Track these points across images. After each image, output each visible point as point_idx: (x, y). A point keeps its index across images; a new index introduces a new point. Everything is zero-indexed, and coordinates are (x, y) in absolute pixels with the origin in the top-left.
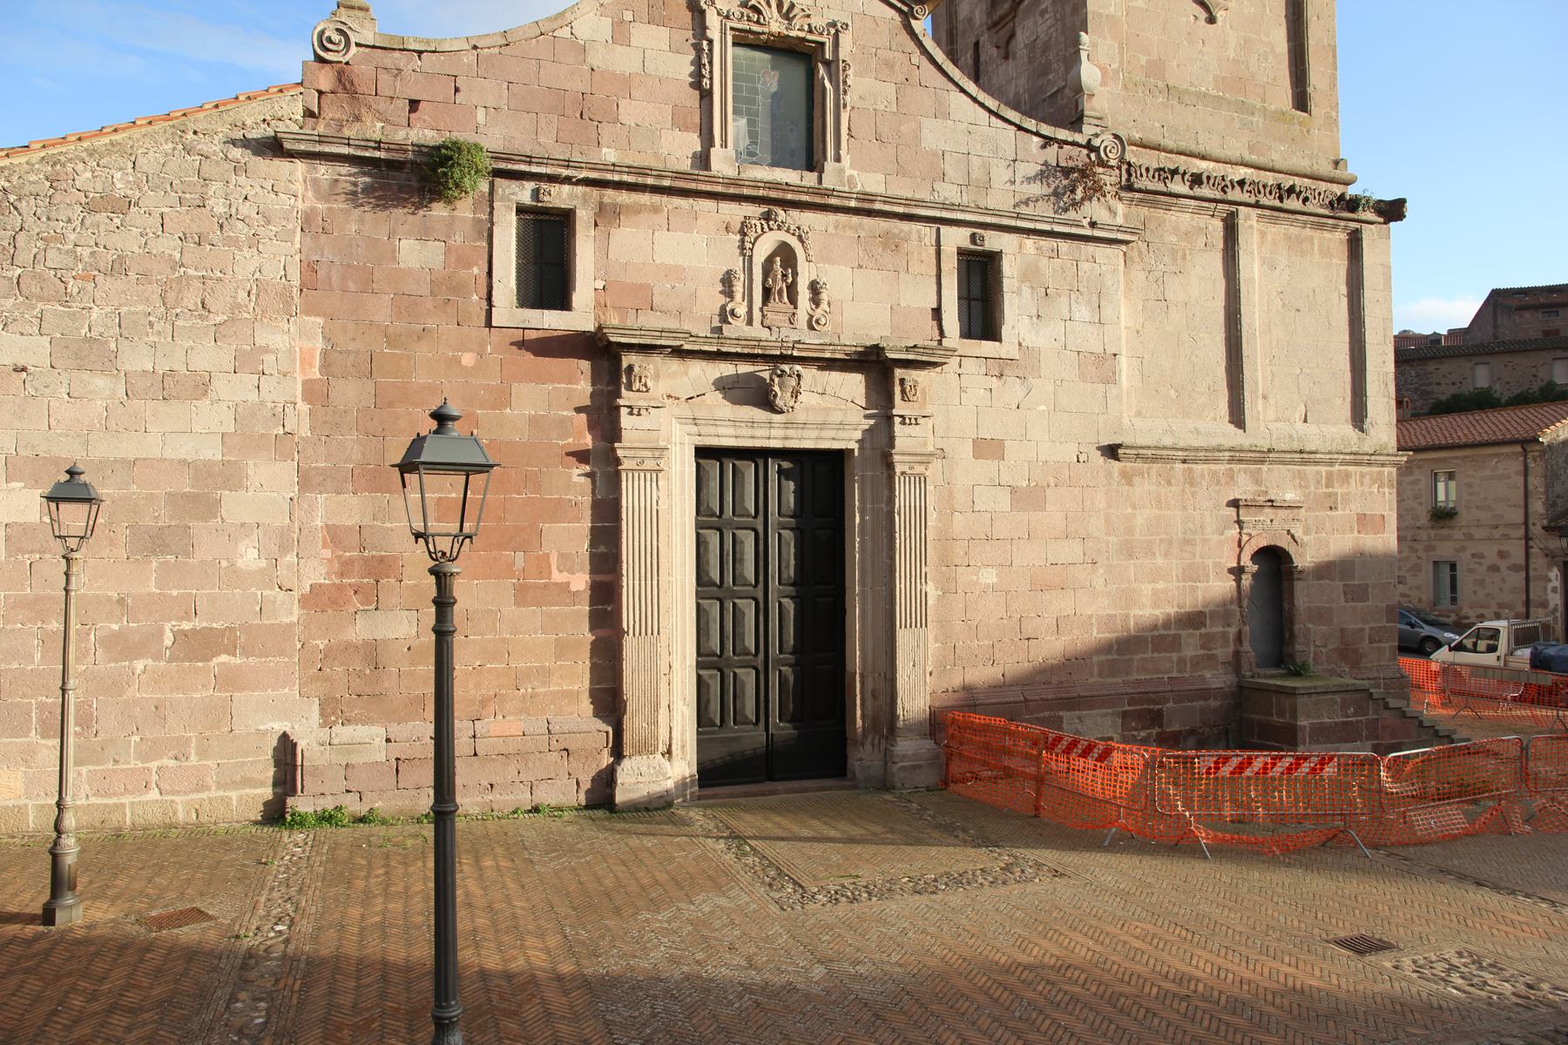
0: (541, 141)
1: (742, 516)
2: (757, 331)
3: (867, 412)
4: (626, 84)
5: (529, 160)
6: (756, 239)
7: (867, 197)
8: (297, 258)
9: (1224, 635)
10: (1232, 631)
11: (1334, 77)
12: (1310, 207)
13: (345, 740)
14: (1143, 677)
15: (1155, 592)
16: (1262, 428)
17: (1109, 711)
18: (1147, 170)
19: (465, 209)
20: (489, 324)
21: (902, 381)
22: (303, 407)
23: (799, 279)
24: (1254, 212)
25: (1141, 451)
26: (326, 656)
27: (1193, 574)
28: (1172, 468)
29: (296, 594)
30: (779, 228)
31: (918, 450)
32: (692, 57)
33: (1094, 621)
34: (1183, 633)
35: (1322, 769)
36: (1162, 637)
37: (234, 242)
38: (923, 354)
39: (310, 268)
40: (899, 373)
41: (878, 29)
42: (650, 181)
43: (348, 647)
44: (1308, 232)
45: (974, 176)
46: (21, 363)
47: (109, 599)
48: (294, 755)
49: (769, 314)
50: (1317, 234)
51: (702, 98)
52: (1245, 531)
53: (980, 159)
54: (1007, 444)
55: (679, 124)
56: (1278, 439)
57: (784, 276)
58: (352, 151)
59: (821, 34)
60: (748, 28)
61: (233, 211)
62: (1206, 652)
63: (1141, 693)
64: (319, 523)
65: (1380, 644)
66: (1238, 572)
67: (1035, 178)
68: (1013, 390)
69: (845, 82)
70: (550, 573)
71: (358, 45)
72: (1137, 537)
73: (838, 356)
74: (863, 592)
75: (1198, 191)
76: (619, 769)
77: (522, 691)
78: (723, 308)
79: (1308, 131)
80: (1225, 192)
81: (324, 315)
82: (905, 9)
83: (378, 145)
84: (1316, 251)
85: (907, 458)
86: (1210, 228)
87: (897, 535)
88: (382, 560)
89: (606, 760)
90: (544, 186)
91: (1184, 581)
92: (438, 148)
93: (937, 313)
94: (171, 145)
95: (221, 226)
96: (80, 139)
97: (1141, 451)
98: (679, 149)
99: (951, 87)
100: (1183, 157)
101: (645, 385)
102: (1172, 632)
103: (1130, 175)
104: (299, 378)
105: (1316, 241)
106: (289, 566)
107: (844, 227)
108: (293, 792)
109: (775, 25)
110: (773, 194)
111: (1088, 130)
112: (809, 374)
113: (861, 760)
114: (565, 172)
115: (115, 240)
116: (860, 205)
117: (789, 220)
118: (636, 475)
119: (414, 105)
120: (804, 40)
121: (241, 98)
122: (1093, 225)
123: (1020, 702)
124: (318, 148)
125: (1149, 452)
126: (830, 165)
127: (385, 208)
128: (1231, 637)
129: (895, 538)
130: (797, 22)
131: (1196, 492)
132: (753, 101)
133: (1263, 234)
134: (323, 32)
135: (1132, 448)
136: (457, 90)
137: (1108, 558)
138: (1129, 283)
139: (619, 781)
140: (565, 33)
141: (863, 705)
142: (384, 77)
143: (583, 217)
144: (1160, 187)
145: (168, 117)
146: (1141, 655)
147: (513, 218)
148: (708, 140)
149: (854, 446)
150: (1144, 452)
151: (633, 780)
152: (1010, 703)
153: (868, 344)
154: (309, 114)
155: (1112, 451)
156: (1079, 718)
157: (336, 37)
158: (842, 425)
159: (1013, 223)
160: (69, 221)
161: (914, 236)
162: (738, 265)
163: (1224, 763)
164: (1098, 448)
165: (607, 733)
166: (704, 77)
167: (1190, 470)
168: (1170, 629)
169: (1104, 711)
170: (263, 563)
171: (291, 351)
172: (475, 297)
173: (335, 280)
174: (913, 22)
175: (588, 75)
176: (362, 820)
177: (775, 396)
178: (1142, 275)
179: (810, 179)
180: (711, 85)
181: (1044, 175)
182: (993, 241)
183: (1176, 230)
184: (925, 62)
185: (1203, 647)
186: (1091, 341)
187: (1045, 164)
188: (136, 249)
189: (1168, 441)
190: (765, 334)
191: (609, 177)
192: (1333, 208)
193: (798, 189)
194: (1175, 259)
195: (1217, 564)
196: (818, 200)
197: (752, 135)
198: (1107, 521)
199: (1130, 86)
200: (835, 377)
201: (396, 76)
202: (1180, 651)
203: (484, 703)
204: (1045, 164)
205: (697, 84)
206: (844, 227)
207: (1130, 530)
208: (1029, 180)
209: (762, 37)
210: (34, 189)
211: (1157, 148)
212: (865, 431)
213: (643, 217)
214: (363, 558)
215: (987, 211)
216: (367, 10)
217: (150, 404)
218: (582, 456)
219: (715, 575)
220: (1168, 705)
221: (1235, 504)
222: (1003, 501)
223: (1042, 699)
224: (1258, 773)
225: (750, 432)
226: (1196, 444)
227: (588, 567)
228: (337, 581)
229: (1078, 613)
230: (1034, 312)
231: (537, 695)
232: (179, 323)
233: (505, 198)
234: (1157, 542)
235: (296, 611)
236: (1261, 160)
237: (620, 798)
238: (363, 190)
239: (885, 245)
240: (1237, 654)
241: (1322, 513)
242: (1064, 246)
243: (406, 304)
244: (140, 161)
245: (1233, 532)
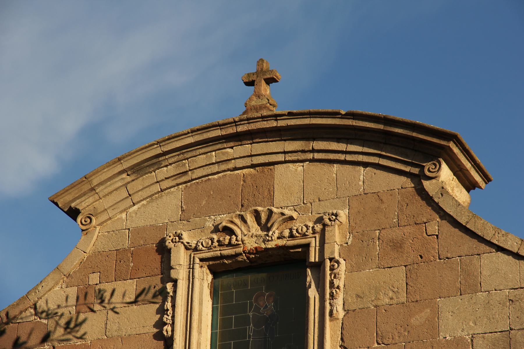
41: (383, 206)
60: (218, 253)
69: (332, 283)
82: (416, 171)
99: (483, 247)
130: (275, 232)
166: (165, 324)
174: (426, 184)
180: (173, 331)
184: (446, 226)
209: (240, 259)
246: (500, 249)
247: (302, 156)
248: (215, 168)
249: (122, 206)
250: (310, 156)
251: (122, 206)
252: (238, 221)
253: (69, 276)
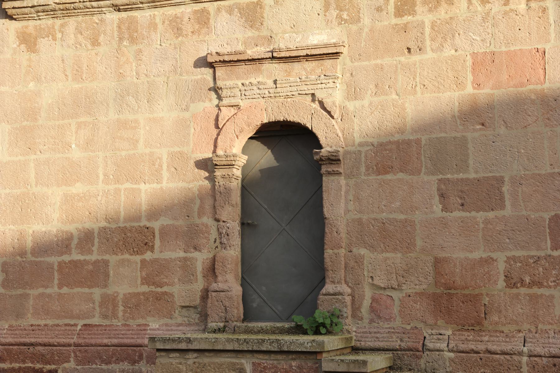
14: (42, 323)
28: (101, 20)
34: (113, 259)
36: (75, 264)
52: (225, 102)
62: (153, 288)
63: (24, 344)
65: (535, 290)
72: (40, 122)
102: (93, 257)
128: (199, 268)
131: (140, 51)
146: (41, 290)
167: (133, 21)
168: (90, 252)
185: (146, 281)
202: (106, 286)
220: (66, 365)
241: (387, 61)
245: (207, 104)
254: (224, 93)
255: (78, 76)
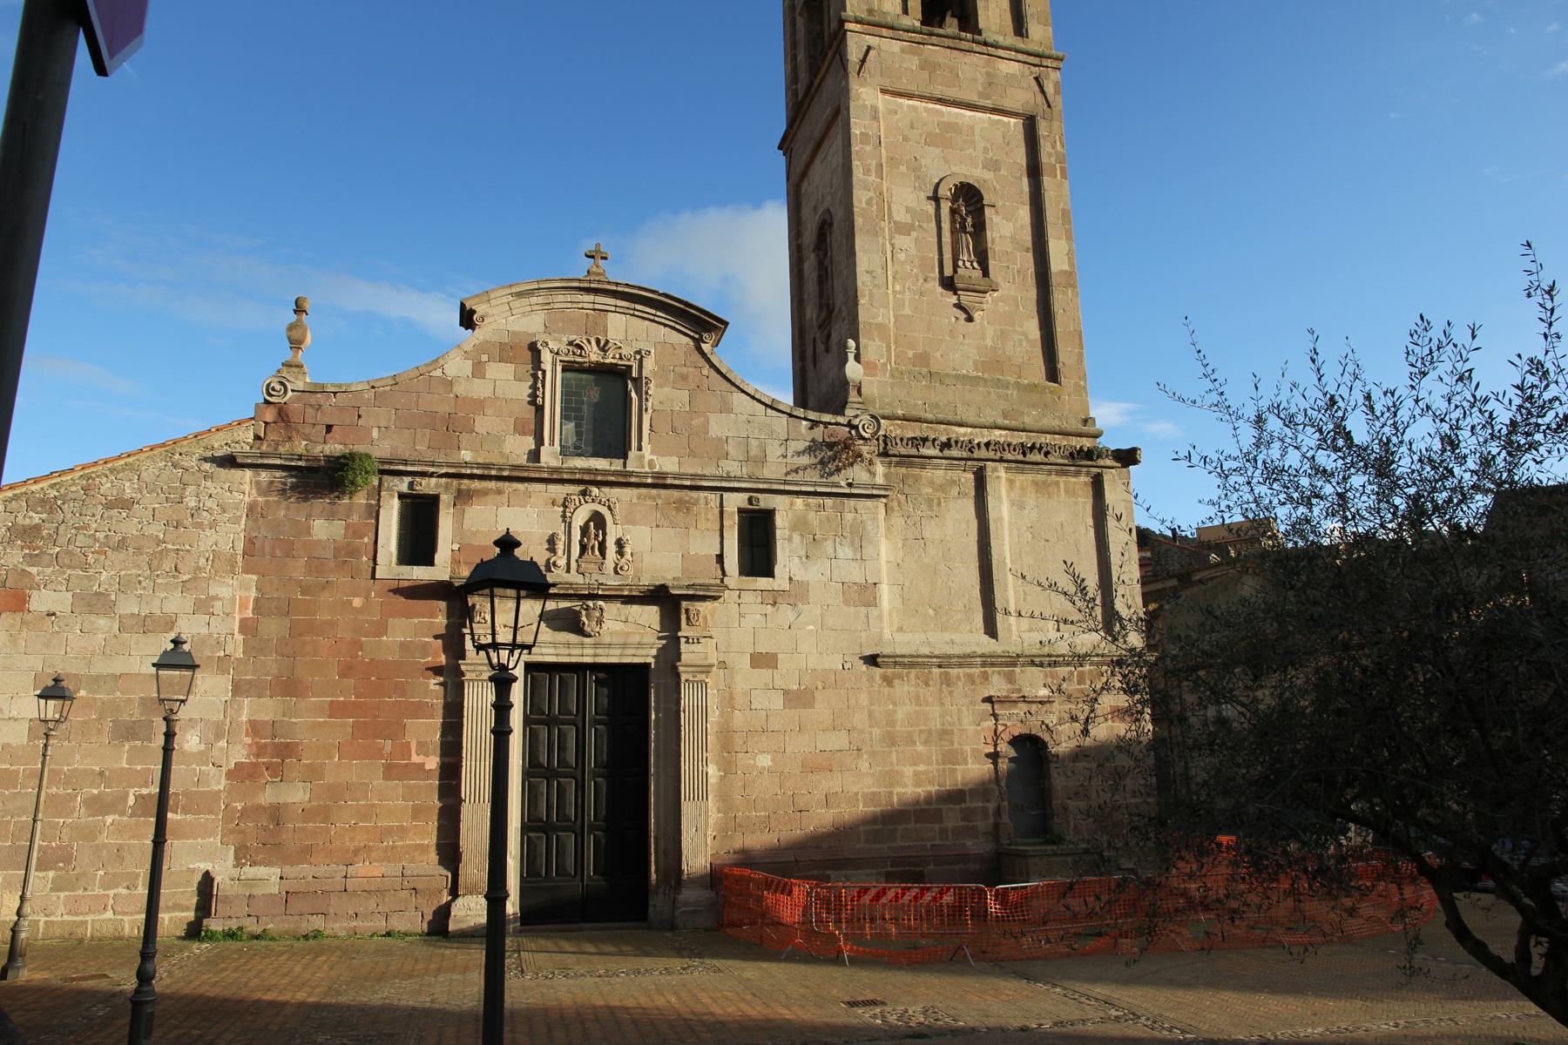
0: (417, 448)
1: (565, 715)
2: (574, 577)
3: (660, 634)
4: (480, 405)
5: (405, 463)
6: (575, 510)
7: (661, 475)
8: (242, 535)
9: (984, 811)
10: (991, 806)
11: (1081, 355)
12: (1051, 459)
13: (249, 877)
15: (916, 774)
16: (1014, 637)
17: (873, 871)
18: (902, 439)
19: (361, 499)
20: (373, 577)
21: (687, 611)
22: (239, 637)
23: (607, 537)
24: (1001, 467)
25: (897, 659)
26: (242, 814)
27: (951, 758)
29: (224, 769)
30: (593, 501)
31: (700, 663)
32: (530, 383)
33: (860, 797)
35: (941, 898)
36: (923, 811)
37: (200, 526)
38: (700, 590)
39: (250, 542)
40: (684, 604)
42: (493, 473)
43: (259, 808)
44: (1054, 478)
45: (752, 454)
46: (52, 611)
47: (93, 771)
48: (212, 887)
49: (583, 565)
50: (1062, 480)
51: (537, 411)
53: (757, 441)
54: (779, 656)
55: (519, 429)
56: (1030, 645)
57: (597, 535)
58: (283, 462)
59: (629, 360)
61: (201, 505)
64: (244, 719)
66: (994, 757)
67: (803, 452)
68: (786, 613)
69: (647, 393)
70: (410, 756)
71: (293, 391)
73: (634, 594)
74: (657, 773)
75: (947, 453)
76: (453, 905)
77: (385, 843)
78: (548, 560)
79: (1059, 398)
80: (972, 452)
81: (258, 574)
82: (697, 336)
83: (300, 458)
84: (1062, 491)
85: (690, 669)
86: (963, 480)
87: (682, 728)
88: (287, 745)
89: (446, 898)
90: (418, 479)
91: (944, 764)
92: (339, 458)
93: (720, 558)
94: (164, 463)
95: (192, 516)
96: (105, 463)
97: (897, 659)
98: (517, 448)
100: (943, 426)
101: (484, 618)
102: (933, 807)
103: (886, 444)
104: (237, 617)
105: (1062, 485)
106: (221, 749)
107: (645, 497)
108: (208, 915)
109: (594, 355)
110: (587, 477)
111: (849, 412)
112: (612, 609)
113: (655, 906)
114: (432, 470)
115: (123, 527)
116: (656, 481)
117: (602, 495)
118: (476, 684)
119: (329, 428)
120: (616, 365)
121: (213, 430)
122: (850, 485)
123: (791, 862)
124: (260, 461)
125: (906, 660)
126: (633, 454)
127: (306, 500)
128: (991, 811)
129: (680, 730)
130: (610, 353)
132: (580, 410)
133: (1011, 482)
134: (269, 385)
135: (889, 657)
136: (359, 416)
137: (872, 746)
138: (889, 529)
139: (452, 914)
140: (438, 373)
141: (656, 861)
142: (310, 411)
143: (445, 499)
144: (914, 451)
145: (163, 446)
147: (396, 503)
148: (539, 441)
149: (651, 660)
150: (901, 660)
151: (463, 913)
152: (782, 863)
153: (657, 583)
154: (257, 437)
155: (872, 660)
156: (846, 877)
157: (278, 387)
158: (640, 645)
159: (782, 487)
160: (93, 515)
161: (702, 501)
162: (561, 530)
163: (865, 893)
164: (860, 658)
165: (447, 877)
169: (868, 871)
170: (202, 747)
171: (233, 600)
172: (365, 559)
173: (267, 549)
174: (703, 345)
175: (453, 401)
176: (257, 937)
177: (584, 624)
178: (901, 521)
179: (617, 465)
180: (543, 402)
181: (813, 448)
182: (766, 501)
183: (931, 483)
184: (713, 373)
185: (963, 819)
186: (855, 574)
187: (813, 440)
188: (135, 533)
189: (925, 650)
190: (580, 579)
191: (463, 471)
192: (1073, 458)
193: (605, 472)
194: (931, 506)
195: (975, 751)
196: (621, 479)
197: (579, 434)
198: (871, 715)
199: (896, 375)
200: (635, 610)
201: (318, 410)
203: (356, 852)
204: (813, 440)
205: (533, 402)
206: (645, 497)
207: (892, 723)
208: (799, 454)
210: (72, 496)
211: (919, 420)
212: (659, 650)
213: (490, 498)
214: (274, 744)
215: (758, 480)
216: (302, 367)
217: (135, 636)
218: (437, 671)
219: (544, 759)
221: (989, 700)
222: (778, 702)
223: (811, 861)
224: (891, 901)
225: (567, 652)
226: (951, 652)
227: (439, 752)
228: (254, 761)
229: (846, 791)
230: (803, 553)
231: (396, 847)
232: (159, 581)
233: (390, 489)
234: (917, 732)
235: (224, 782)
236: (1014, 424)
237: (452, 927)
238: (291, 488)
239: (678, 509)
240: (996, 825)
242: (829, 502)
243: (316, 565)
244: (144, 474)
245: (990, 723)
246: (743, 391)
247: (627, 311)
248: (569, 305)
249: (504, 315)
250: (632, 312)
251: (504, 315)
252: (585, 342)
253: (466, 352)
254: (1000, 717)
255: (918, 703)
